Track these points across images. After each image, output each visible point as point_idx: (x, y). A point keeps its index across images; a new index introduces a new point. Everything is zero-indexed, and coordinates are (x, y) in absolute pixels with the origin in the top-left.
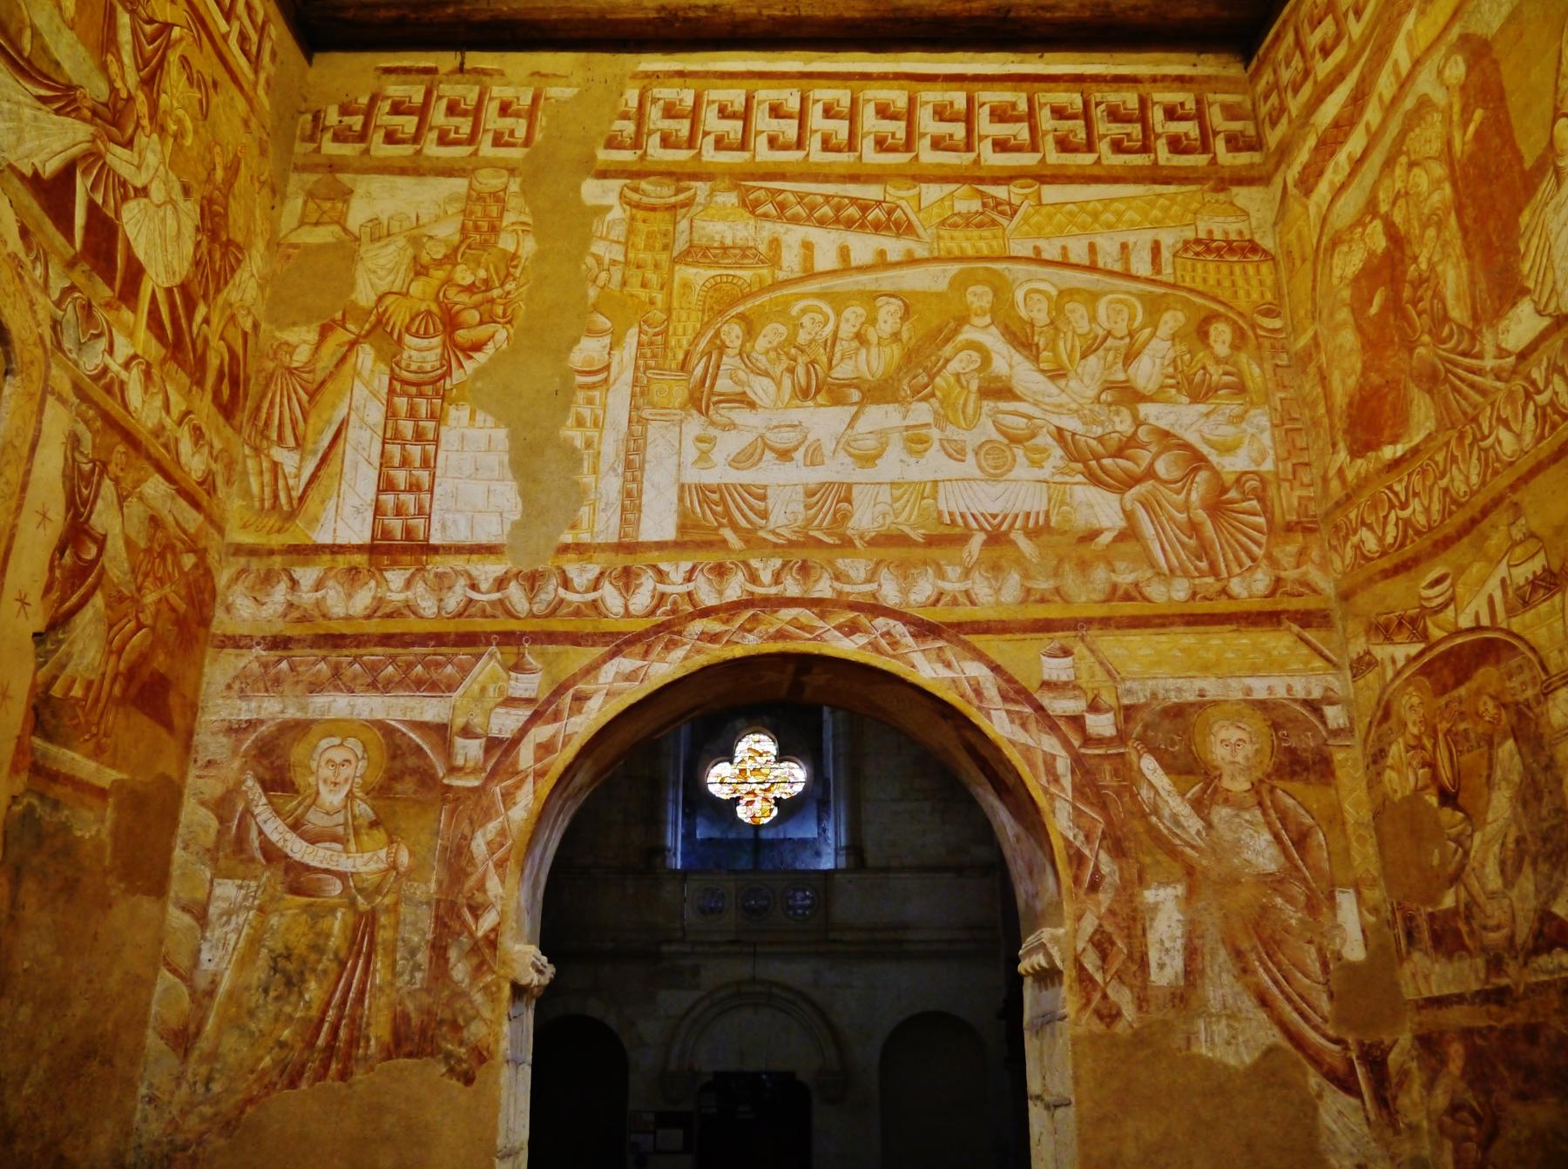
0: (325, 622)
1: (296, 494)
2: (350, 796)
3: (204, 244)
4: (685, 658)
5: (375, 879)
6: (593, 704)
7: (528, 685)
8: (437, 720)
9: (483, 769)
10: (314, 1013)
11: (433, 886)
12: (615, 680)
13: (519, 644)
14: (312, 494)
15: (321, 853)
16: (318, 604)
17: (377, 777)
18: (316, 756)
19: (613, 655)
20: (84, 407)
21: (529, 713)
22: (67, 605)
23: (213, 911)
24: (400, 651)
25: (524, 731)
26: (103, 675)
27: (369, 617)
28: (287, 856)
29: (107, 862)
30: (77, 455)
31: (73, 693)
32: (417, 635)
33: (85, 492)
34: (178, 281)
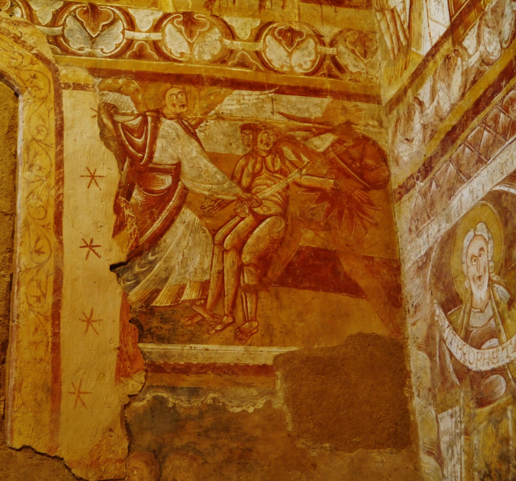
1: (406, 26)
14: (412, 17)
20: (110, 81)
22: (149, 233)
26: (221, 273)
29: (290, 428)
30: (118, 118)
33: (139, 141)
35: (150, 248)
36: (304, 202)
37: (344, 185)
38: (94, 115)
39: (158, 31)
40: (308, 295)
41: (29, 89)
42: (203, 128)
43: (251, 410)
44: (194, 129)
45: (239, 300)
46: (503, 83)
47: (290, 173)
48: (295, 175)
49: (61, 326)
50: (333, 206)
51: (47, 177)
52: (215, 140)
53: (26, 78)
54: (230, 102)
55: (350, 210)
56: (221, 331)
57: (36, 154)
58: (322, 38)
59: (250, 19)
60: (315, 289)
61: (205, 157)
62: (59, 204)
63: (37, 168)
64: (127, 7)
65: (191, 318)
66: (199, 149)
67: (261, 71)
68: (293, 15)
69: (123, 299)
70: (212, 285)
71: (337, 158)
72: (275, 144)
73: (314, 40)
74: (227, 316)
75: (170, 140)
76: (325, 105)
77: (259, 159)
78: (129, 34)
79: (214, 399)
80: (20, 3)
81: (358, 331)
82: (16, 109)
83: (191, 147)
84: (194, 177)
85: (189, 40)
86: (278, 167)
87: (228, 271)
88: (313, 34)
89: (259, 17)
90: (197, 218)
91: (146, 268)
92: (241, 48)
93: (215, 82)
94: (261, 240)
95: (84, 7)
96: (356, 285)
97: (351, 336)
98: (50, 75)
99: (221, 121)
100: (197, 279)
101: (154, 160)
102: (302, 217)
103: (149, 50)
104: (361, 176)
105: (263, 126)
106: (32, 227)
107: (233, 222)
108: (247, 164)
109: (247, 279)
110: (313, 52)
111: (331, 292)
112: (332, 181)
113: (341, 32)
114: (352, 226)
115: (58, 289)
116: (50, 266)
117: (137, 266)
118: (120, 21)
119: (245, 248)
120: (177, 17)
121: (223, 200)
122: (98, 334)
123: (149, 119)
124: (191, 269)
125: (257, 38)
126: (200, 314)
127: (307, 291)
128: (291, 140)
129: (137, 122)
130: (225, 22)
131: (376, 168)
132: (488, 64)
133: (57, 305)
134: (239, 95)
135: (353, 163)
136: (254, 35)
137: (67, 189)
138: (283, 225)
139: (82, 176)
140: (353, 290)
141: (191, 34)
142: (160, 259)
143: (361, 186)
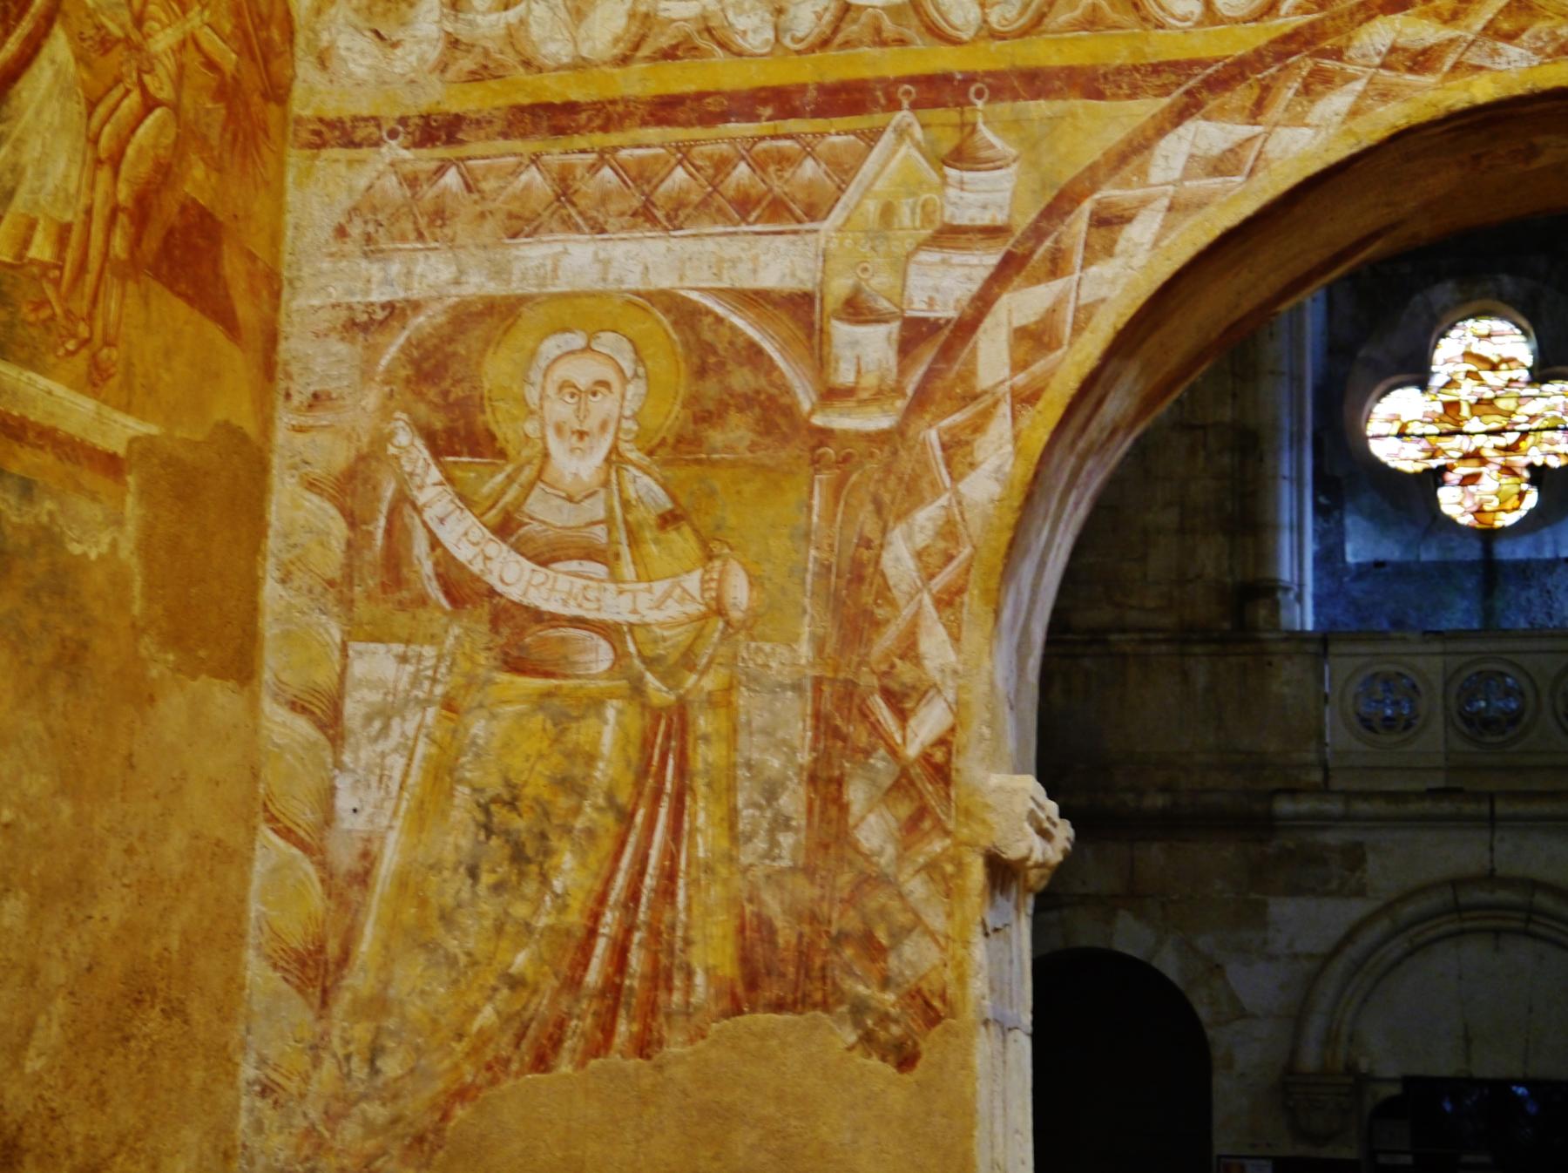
0: (530, 78)
2: (614, 459)
4: (1354, 113)
5: (681, 636)
6: (1140, 233)
7: (990, 196)
8: (791, 285)
9: (899, 390)
10: (575, 918)
11: (805, 650)
12: (1187, 174)
13: (962, 102)
15: (563, 583)
16: (512, 36)
17: (670, 416)
18: (536, 376)
19: (1181, 115)
21: (993, 259)
23: (353, 709)
24: (698, 132)
25: (983, 302)
26: (89, 212)
27: (624, 60)
28: (492, 592)
29: (137, 608)
31: (33, 253)
32: (733, 96)
43: (93, 555)
46: (768, 111)
79: (51, 514)
132: (723, 45)
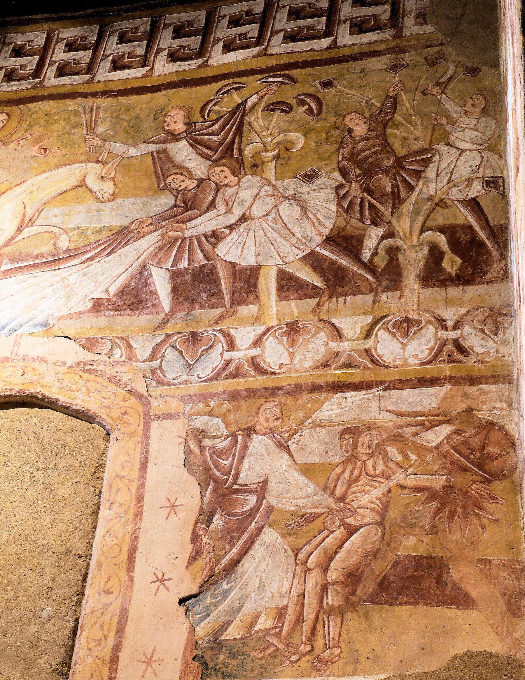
3: (355, 190)
26: (302, 596)
30: (207, 442)
34: (318, 240)
35: (226, 575)
36: (407, 506)
37: (460, 480)
38: (180, 442)
39: (258, 346)
40: (404, 611)
41: (119, 426)
42: (297, 440)
44: (286, 442)
45: (320, 625)
47: (394, 475)
48: (399, 477)
49: (119, 670)
50: (443, 505)
51: (126, 513)
52: (309, 451)
53: (117, 416)
54: (329, 408)
55: (464, 508)
56: (296, 662)
57: (118, 491)
58: (444, 323)
59: (361, 316)
60: (415, 604)
61: (296, 470)
62: (135, 539)
63: (118, 504)
64: (229, 328)
65: (265, 649)
66: (290, 462)
67: (369, 368)
68: (411, 304)
69: (189, 635)
70: (290, 611)
71: (451, 450)
72: (378, 445)
73: (435, 327)
74: (305, 644)
75: (258, 457)
76: (442, 394)
77: (359, 464)
78: (228, 355)
80: (121, 344)
81: (465, 649)
82: (105, 449)
83: (281, 461)
84: (281, 494)
85: (291, 350)
86: (380, 469)
87: (309, 593)
88: (434, 320)
89: (370, 313)
90: (279, 537)
91: (219, 598)
92: (348, 349)
93: (315, 388)
94: (352, 554)
95: (185, 336)
96: (467, 595)
97: (456, 657)
98: (141, 409)
99: (318, 429)
100: (274, 605)
101: (240, 481)
102: (403, 522)
103: (246, 367)
104: (481, 467)
105: (366, 428)
106: (104, 567)
107: (320, 537)
108: (344, 471)
109: (332, 599)
110: (433, 339)
111: (433, 605)
112: (444, 477)
113: (468, 312)
114: (466, 527)
115: (120, 631)
116: (116, 607)
117: (209, 597)
118: (220, 344)
119: (332, 565)
120: (279, 329)
121: (311, 514)
122: (156, 675)
123: (240, 438)
124: (268, 594)
125: (368, 335)
126: (274, 644)
127: (403, 607)
128: (397, 439)
129: (226, 443)
130: (333, 325)
131: (501, 456)
133: (117, 647)
134: (342, 398)
135: (472, 454)
136: (365, 332)
137: (144, 523)
138: (379, 534)
139: (162, 508)
140: (461, 600)
141: (293, 343)
142: (236, 587)
143: (481, 479)
